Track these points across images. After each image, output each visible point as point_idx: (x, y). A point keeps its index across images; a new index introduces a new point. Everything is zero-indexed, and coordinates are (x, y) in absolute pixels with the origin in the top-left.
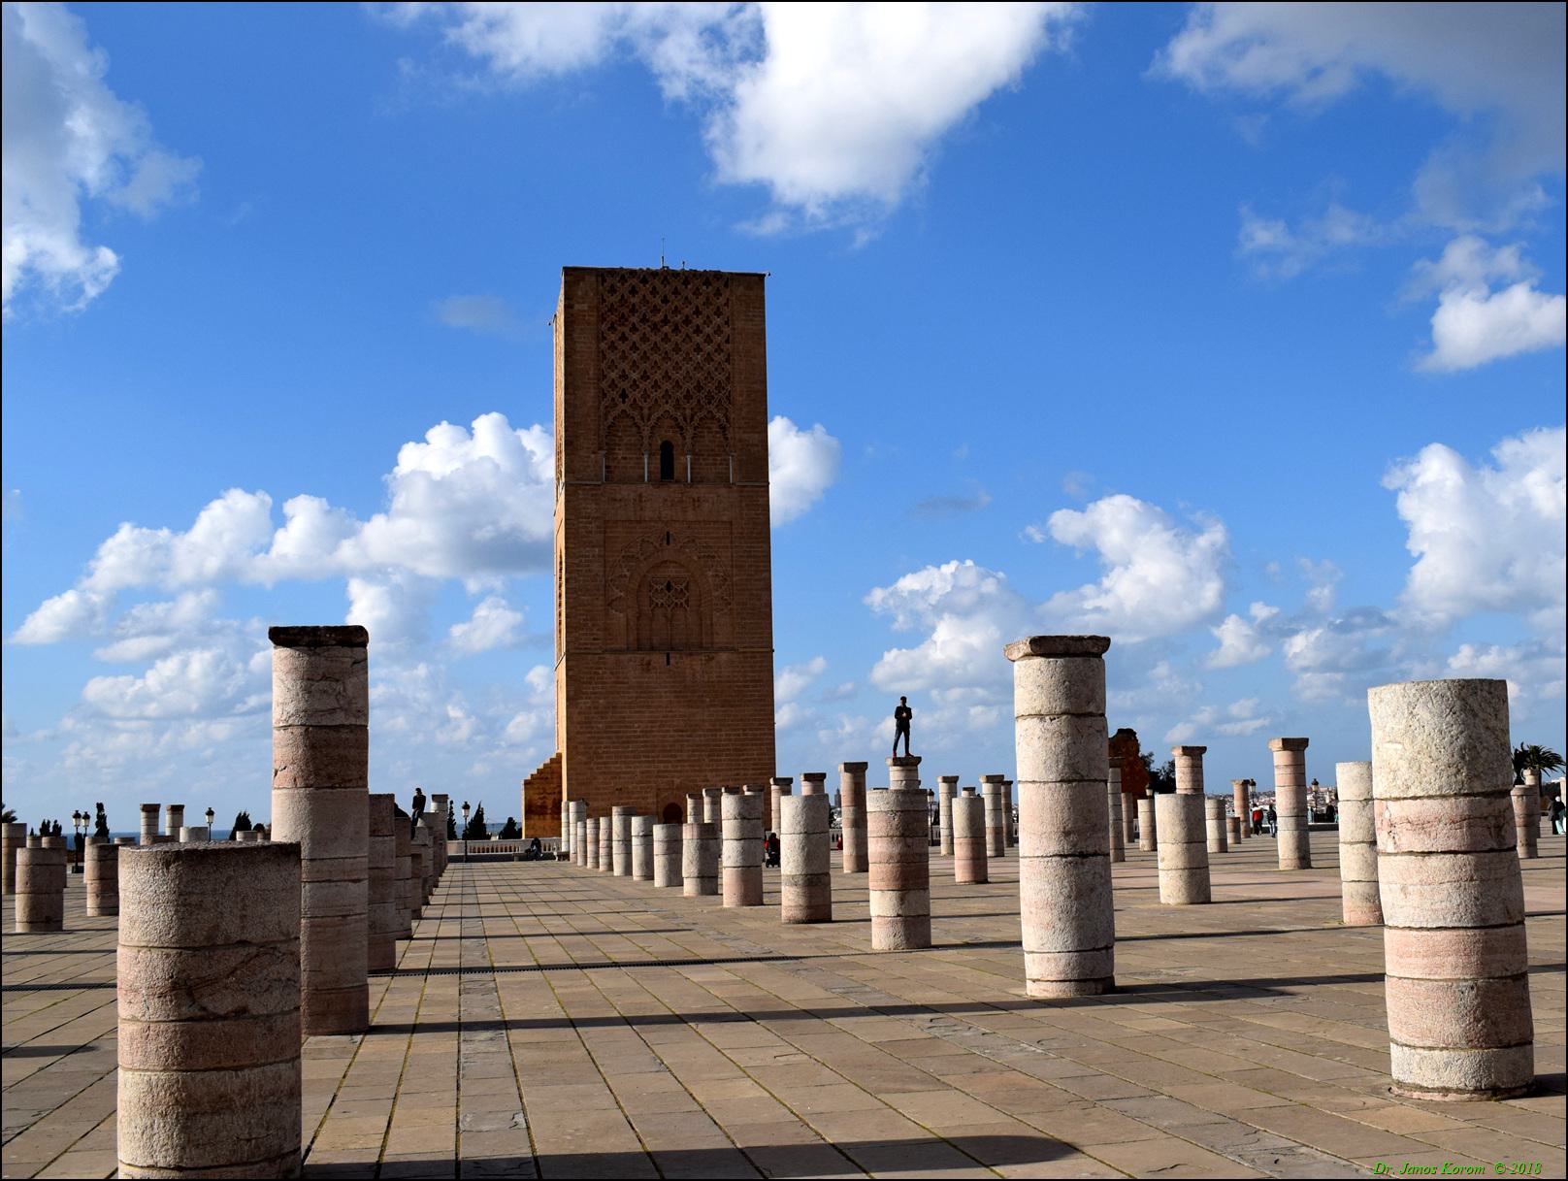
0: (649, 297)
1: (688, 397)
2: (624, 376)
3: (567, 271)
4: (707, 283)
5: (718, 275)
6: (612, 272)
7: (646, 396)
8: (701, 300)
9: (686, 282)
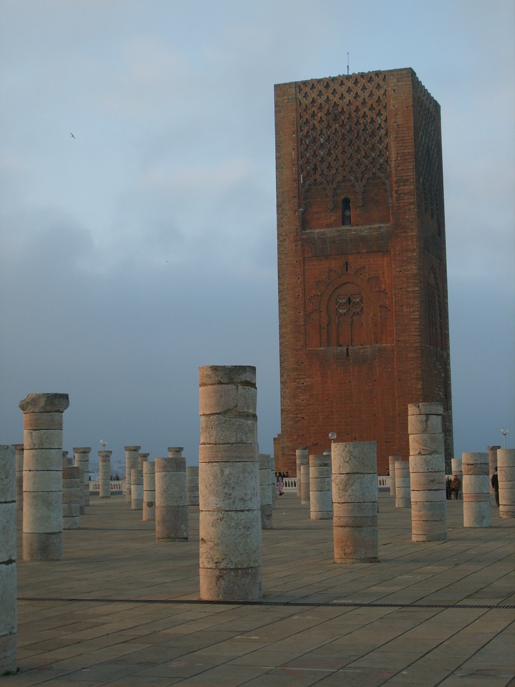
0: (331, 97)
1: (359, 163)
2: (315, 155)
3: (277, 87)
4: (370, 80)
5: (377, 74)
6: (305, 83)
7: (329, 167)
8: (367, 93)
9: (356, 82)
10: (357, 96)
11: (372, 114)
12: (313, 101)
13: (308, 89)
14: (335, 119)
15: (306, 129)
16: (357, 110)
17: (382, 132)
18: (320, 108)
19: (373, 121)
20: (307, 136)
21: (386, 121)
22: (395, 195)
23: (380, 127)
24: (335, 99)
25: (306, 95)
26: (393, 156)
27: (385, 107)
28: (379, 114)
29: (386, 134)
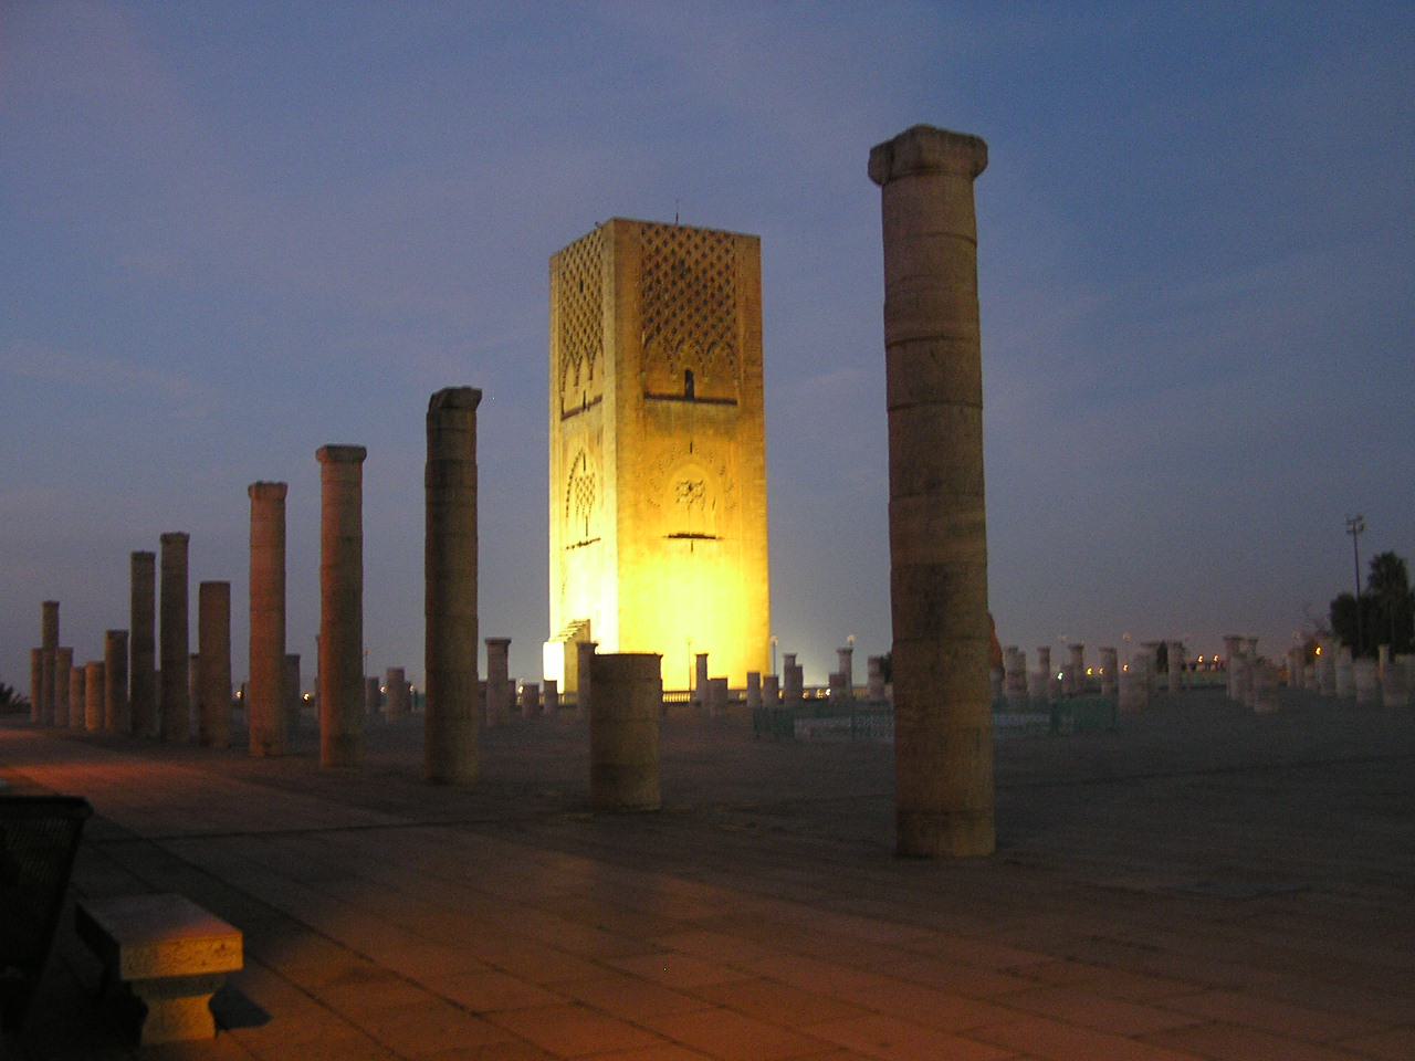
9: (704, 239)
10: (704, 256)
11: (719, 281)
12: (658, 250)
13: (651, 233)
14: (682, 277)
15: (648, 280)
16: (705, 272)
17: (731, 302)
18: (665, 259)
19: (720, 288)
20: (650, 288)
21: (734, 289)
22: (743, 375)
23: (728, 297)
24: (682, 253)
25: (650, 242)
26: (742, 331)
27: (734, 275)
28: (728, 282)
29: (734, 305)
